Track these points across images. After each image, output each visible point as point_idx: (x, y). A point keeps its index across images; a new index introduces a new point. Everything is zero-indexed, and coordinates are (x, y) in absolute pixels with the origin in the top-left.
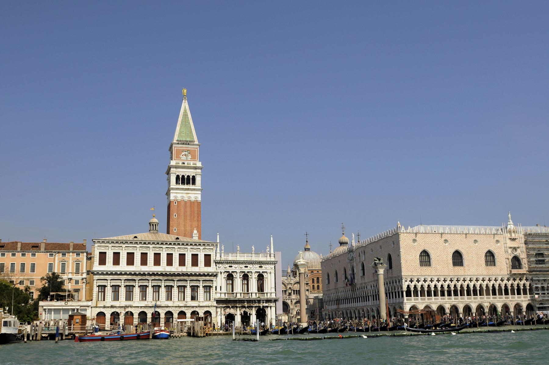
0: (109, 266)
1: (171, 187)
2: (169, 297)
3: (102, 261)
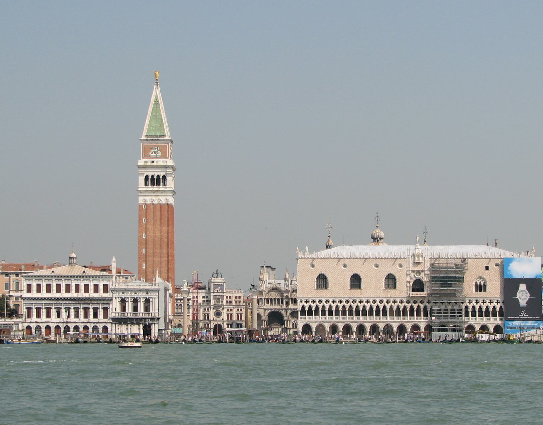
0: (34, 294)
1: (140, 189)
2: (77, 316)
3: (29, 290)
